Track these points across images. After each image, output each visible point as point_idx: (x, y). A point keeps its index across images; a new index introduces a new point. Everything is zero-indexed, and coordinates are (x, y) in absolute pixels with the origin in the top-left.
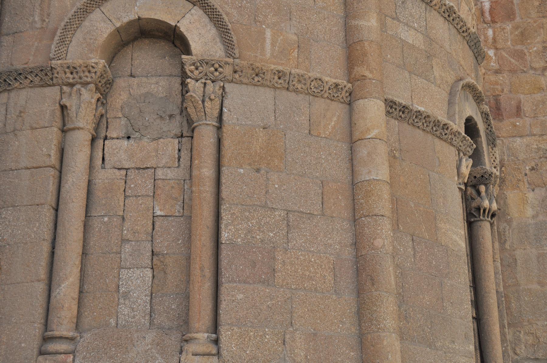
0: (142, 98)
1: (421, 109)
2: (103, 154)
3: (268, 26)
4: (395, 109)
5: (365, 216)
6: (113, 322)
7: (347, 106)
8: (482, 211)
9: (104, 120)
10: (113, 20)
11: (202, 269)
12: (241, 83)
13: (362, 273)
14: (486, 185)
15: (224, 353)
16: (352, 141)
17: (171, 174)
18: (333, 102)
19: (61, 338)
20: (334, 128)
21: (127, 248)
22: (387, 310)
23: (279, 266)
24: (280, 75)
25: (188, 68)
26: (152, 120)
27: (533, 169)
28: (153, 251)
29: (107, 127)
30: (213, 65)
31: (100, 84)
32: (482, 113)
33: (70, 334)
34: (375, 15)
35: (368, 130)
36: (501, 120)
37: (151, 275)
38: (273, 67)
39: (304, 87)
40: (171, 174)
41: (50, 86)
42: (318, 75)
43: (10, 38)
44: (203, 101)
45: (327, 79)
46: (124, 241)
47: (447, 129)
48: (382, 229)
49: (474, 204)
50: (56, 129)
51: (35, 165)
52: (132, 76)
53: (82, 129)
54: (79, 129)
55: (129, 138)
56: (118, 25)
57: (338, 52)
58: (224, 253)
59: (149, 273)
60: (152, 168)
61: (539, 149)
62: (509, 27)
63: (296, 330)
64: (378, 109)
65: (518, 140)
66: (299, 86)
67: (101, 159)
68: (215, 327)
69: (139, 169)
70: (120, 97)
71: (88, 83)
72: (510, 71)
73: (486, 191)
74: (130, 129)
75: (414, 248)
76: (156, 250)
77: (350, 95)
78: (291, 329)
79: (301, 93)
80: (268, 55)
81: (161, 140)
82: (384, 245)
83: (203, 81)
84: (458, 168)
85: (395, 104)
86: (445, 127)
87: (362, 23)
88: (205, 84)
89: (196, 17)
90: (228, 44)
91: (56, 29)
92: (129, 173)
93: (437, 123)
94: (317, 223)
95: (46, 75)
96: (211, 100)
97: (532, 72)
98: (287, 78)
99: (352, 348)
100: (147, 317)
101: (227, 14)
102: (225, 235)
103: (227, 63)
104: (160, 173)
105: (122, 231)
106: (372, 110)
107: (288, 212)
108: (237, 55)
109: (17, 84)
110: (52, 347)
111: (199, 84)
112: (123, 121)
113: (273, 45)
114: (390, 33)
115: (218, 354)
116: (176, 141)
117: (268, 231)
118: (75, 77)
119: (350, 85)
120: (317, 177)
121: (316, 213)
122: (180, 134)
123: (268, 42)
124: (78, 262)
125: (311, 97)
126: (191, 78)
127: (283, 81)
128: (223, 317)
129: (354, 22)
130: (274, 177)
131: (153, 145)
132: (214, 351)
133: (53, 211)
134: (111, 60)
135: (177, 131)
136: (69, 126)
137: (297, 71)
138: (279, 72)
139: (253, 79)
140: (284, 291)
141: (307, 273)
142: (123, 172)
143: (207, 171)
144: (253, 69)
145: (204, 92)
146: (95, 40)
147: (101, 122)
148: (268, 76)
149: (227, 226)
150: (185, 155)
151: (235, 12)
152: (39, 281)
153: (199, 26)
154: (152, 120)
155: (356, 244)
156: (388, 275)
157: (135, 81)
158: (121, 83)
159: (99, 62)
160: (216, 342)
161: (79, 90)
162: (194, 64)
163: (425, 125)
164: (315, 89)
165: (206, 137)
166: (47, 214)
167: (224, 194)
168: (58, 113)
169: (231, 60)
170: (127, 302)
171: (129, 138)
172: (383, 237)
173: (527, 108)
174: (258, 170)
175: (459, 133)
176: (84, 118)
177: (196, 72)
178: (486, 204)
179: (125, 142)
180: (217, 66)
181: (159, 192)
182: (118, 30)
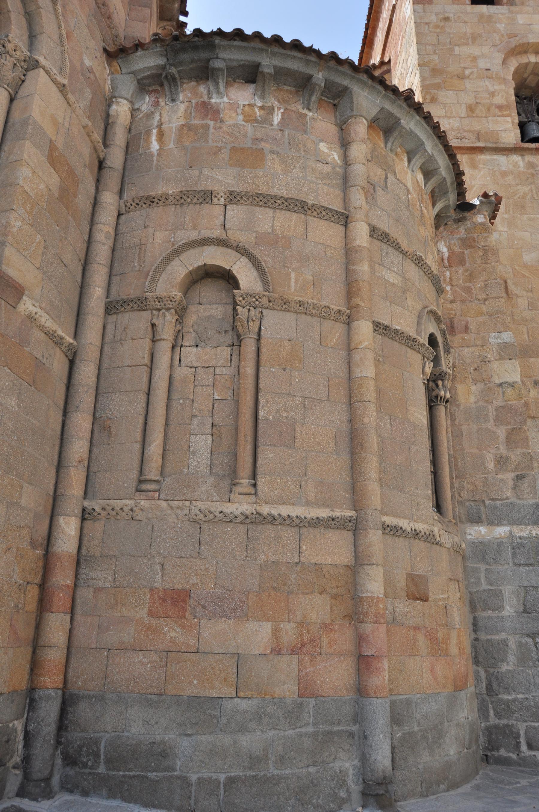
0: (207, 319)
1: (398, 327)
2: (180, 357)
3: (293, 270)
4: (380, 328)
5: (358, 402)
6: (185, 470)
7: (347, 326)
8: (439, 398)
9: (181, 334)
10: (188, 266)
11: (245, 436)
12: (274, 309)
13: (354, 441)
14: (442, 380)
15: (260, 493)
16: (350, 349)
17: (226, 371)
18: (337, 323)
19: (150, 481)
20: (337, 340)
21: (195, 421)
22: (372, 467)
23: (298, 435)
24: (301, 304)
25: (238, 299)
26: (213, 334)
27: (475, 369)
28: (212, 424)
29: (183, 339)
30: (255, 297)
31: (178, 309)
32: (441, 330)
33: (157, 478)
34: (367, 262)
35: (361, 342)
36: (454, 335)
37: (211, 440)
38: (296, 298)
39: (317, 312)
40: (225, 371)
41: (145, 310)
42: (327, 304)
43: (118, 278)
44: (248, 322)
45: (333, 307)
46: (194, 416)
47: (416, 341)
48: (369, 411)
49: (434, 394)
50: (148, 340)
51: (134, 364)
52: (200, 304)
53: (166, 340)
54: (163, 340)
55: (197, 346)
56: (191, 269)
57: (340, 288)
58: (261, 425)
59: (210, 438)
60: (213, 367)
61: (480, 356)
62: (461, 270)
63: (309, 479)
64: (368, 328)
65: (466, 349)
66: (314, 312)
67: (178, 361)
68: (254, 475)
69: (204, 367)
70: (191, 319)
71: (170, 309)
72: (461, 301)
73: (443, 385)
74: (198, 340)
75: (391, 424)
76: (215, 422)
77: (349, 318)
78: (305, 478)
79: (315, 316)
80: (293, 290)
81: (219, 348)
82: (370, 422)
83: (248, 307)
84: (423, 369)
85: (380, 324)
86: (415, 340)
87: (358, 268)
88: (249, 310)
89: (243, 264)
91: (149, 271)
92: (197, 370)
93: (409, 338)
94: (324, 406)
95: (142, 303)
96: (253, 321)
97: (476, 302)
98: (305, 306)
99: (347, 492)
100: (208, 468)
101: (265, 262)
102: (261, 414)
103: (264, 295)
104: (218, 371)
105: (192, 409)
107: (305, 398)
108: (271, 290)
109: (122, 309)
110: (145, 486)
111: (245, 310)
112: (194, 335)
113: (296, 283)
114: (378, 275)
115: (256, 494)
116: (229, 348)
117: (291, 411)
118: (161, 305)
119: (349, 311)
120: (325, 375)
121: (324, 399)
122: (232, 344)
123: (293, 281)
124: (162, 430)
125: (322, 319)
126: (239, 305)
127: (303, 308)
128: (259, 469)
129: (352, 268)
130: (295, 374)
131: (214, 351)
132: (253, 492)
133: (146, 396)
134: (185, 293)
135: (230, 342)
136: (157, 337)
137: (313, 301)
138: (300, 302)
139: (282, 306)
140: (301, 452)
141: (317, 440)
142: (193, 369)
143: (249, 370)
144: (282, 300)
145: (248, 315)
146: (175, 279)
147: (178, 335)
148: (293, 304)
149: (262, 407)
150: (235, 358)
151: (270, 260)
152: (136, 442)
153: (245, 270)
154: (213, 334)
155: (351, 421)
156: (373, 442)
157: (202, 307)
158: (192, 308)
159: (177, 294)
160: (255, 485)
161: (164, 313)
162: (241, 296)
163: (401, 339)
164: (324, 314)
165: (249, 346)
166: (142, 398)
167: (261, 385)
168: (150, 329)
169: (267, 293)
170: (195, 457)
171: (197, 346)
172: (370, 416)
173: (472, 327)
174: (284, 369)
175: (424, 345)
176: (167, 333)
177: (243, 302)
178: (442, 393)
179: (195, 349)
180: (258, 297)
181: (217, 383)
182: (190, 272)
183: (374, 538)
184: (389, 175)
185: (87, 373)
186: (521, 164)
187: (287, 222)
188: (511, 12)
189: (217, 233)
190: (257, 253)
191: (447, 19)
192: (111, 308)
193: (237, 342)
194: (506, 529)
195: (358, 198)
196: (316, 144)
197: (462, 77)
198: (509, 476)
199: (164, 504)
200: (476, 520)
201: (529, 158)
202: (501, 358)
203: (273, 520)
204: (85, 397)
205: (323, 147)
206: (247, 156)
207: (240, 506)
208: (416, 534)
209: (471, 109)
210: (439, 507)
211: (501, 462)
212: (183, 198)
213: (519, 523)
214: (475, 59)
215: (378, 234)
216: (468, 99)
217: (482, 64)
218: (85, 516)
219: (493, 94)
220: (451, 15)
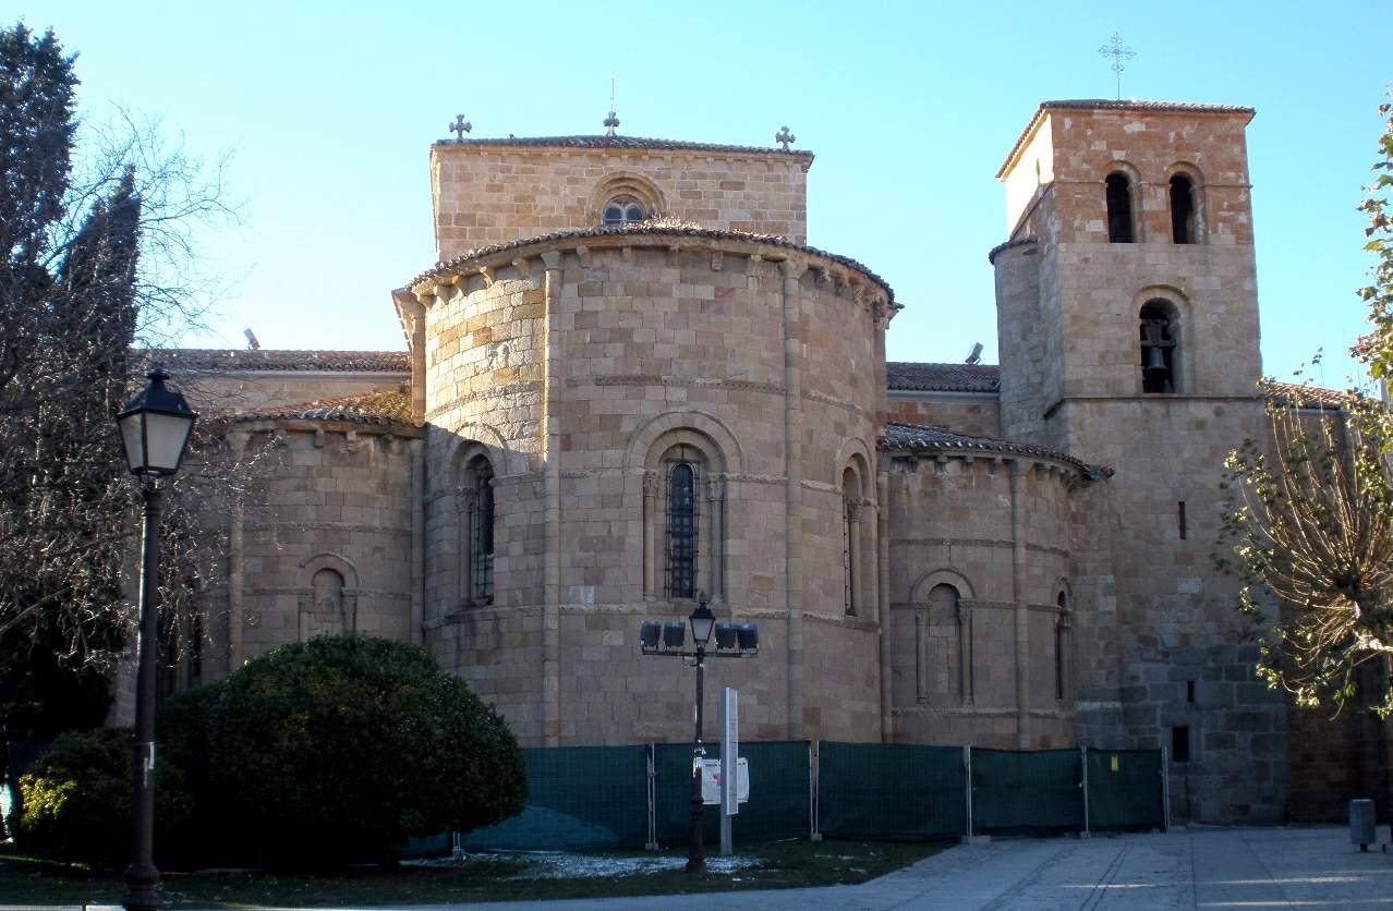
4: (1031, 608)
17: (953, 639)
22: (1025, 685)
68: (972, 694)
90: (974, 594)
102: (974, 663)
106: (1023, 614)
110: (921, 701)
118: (921, 606)
143: (966, 640)
156: (1026, 675)
164: (1003, 606)
172: (1025, 661)
173: (1089, 570)
183: (1026, 721)
184: (1038, 499)
185: (887, 644)
186: (1139, 410)
187: (983, 554)
188: (1141, 250)
189: (945, 564)
190: (967, 575)
191: (1086, 260)
192: (893, 606)
193: (959, 623)
194: (1099, 703)
195: (1020, 532)
196: (997, 496)
197: (1097, 323)
198: (1104, 672)
199: (932, 710)
200: (1083, 698)
201: (1146, 405)
202: (1105, 595)
203: (981, 715)
204: (888, 658)
205: (1000, 497)
206: (960, 513)
207: (966, 710)
208: (1046, 716)
209: (1102, 356)
210: (1060, 694)
211: (1100, 663)
212: (925, 542)
213: (1107, 700)
214: (1108, 303)
215: (1029, 547)
217: (1115, 309)
218: (894, 714)
219: (1120, 341)
220: (1090, 256)
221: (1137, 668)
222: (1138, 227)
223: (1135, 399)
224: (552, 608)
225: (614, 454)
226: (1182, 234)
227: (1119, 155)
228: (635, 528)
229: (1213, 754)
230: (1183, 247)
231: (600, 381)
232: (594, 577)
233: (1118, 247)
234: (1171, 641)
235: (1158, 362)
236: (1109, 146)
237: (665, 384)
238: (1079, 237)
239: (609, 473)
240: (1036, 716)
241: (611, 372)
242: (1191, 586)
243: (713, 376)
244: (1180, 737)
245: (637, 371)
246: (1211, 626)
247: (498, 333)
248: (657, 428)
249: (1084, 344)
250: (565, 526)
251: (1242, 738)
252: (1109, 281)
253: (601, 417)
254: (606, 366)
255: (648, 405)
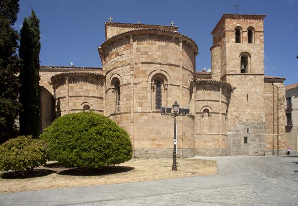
4: (222, 114)
16: (219, 117)
106: (220, 114)
191: (231, 46)
197: (233, 59)
209: (234, 66)
215: (222, 102)
216: (233, 64)
217: (236, 56)
219: (237, 63)
221: (238, 126)
222: (241, 40)
223: (240, 75)
224: (132, 112)
225: (145, 79)
226: (250, 41)
227: (238, 25)
228: (149, 94)
229: (252, 142)
230: (250, 44)
231: (142, 63)
232: (141, 105)
233: (237, 44)
234: (245, 121)
235: (243, 68)
236: (237, 23)
237: (156, 64)
238: (230, 42)
239: (143, 83)
240: (222, 135)
241: (144, 61)
242: (249, 110)
243: (165, 62)
244: (246, 139)
245: (149, 61)
246: (252, 118)
247: (120, 54)
248: (154, 73)
249: (230, 63)
250: (135, 94)
251: (257, 140)
252: (236, 50)
253: (142, 71)
254: (143, 60)
255: (152, 67)
